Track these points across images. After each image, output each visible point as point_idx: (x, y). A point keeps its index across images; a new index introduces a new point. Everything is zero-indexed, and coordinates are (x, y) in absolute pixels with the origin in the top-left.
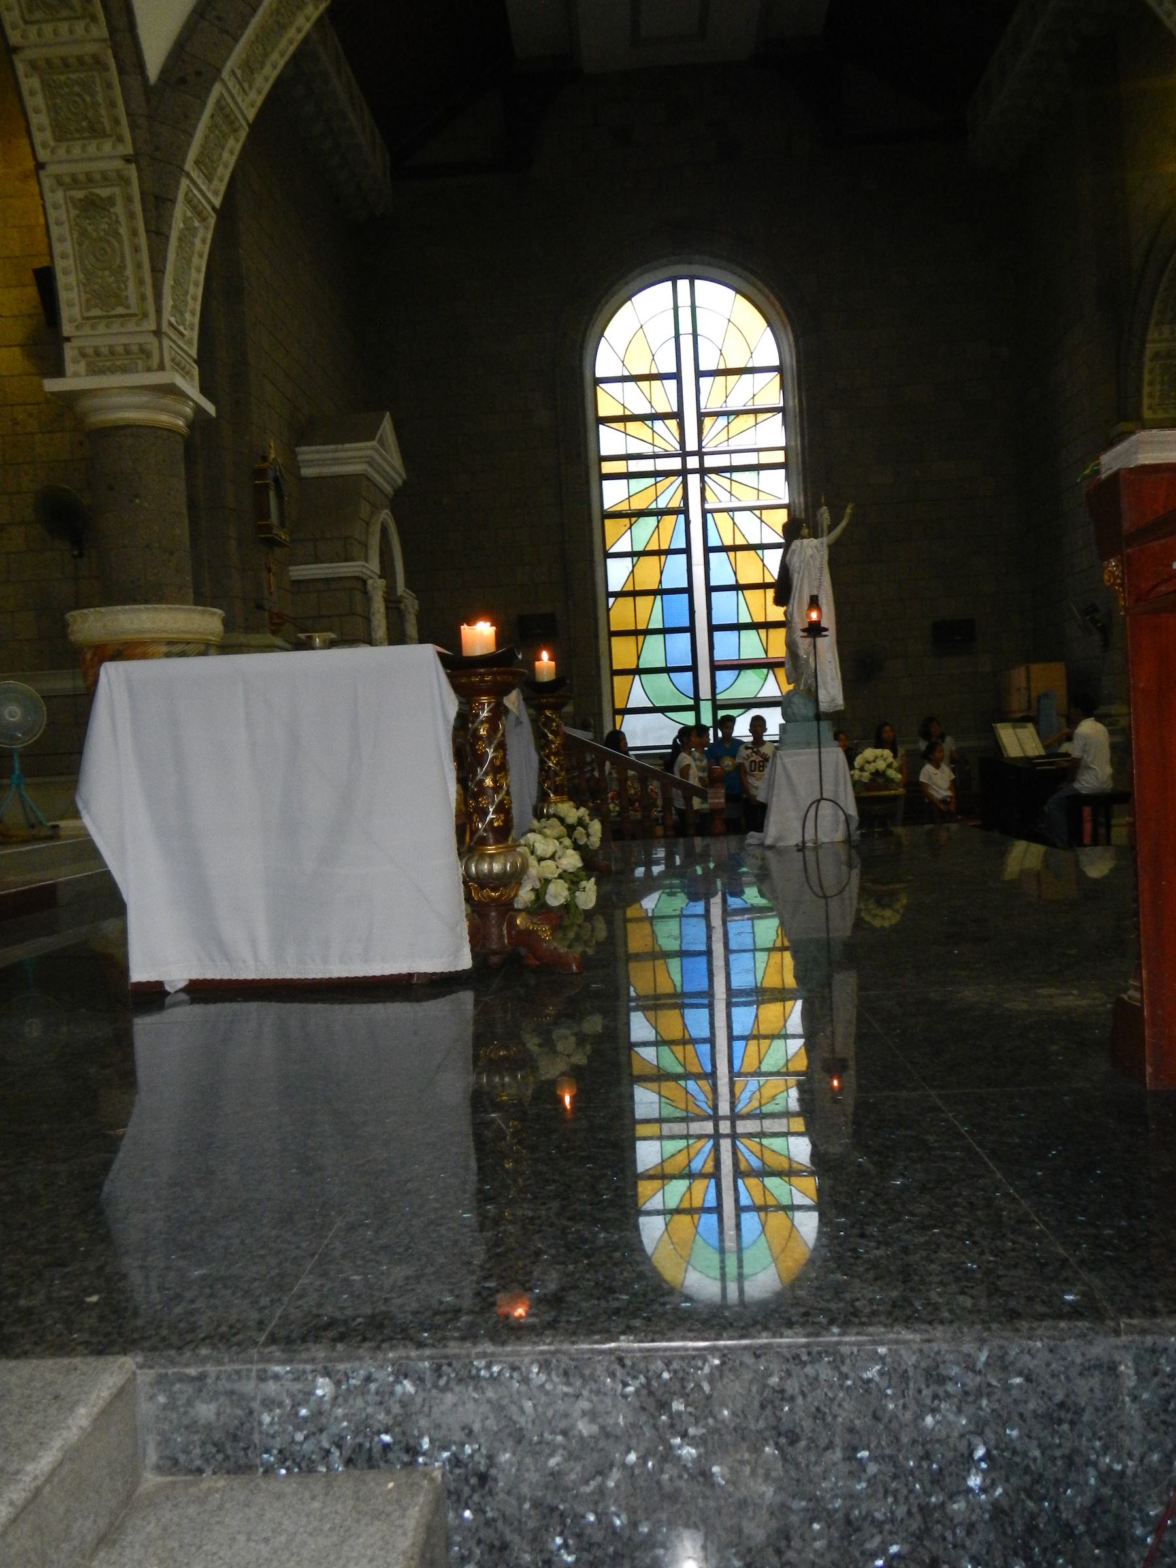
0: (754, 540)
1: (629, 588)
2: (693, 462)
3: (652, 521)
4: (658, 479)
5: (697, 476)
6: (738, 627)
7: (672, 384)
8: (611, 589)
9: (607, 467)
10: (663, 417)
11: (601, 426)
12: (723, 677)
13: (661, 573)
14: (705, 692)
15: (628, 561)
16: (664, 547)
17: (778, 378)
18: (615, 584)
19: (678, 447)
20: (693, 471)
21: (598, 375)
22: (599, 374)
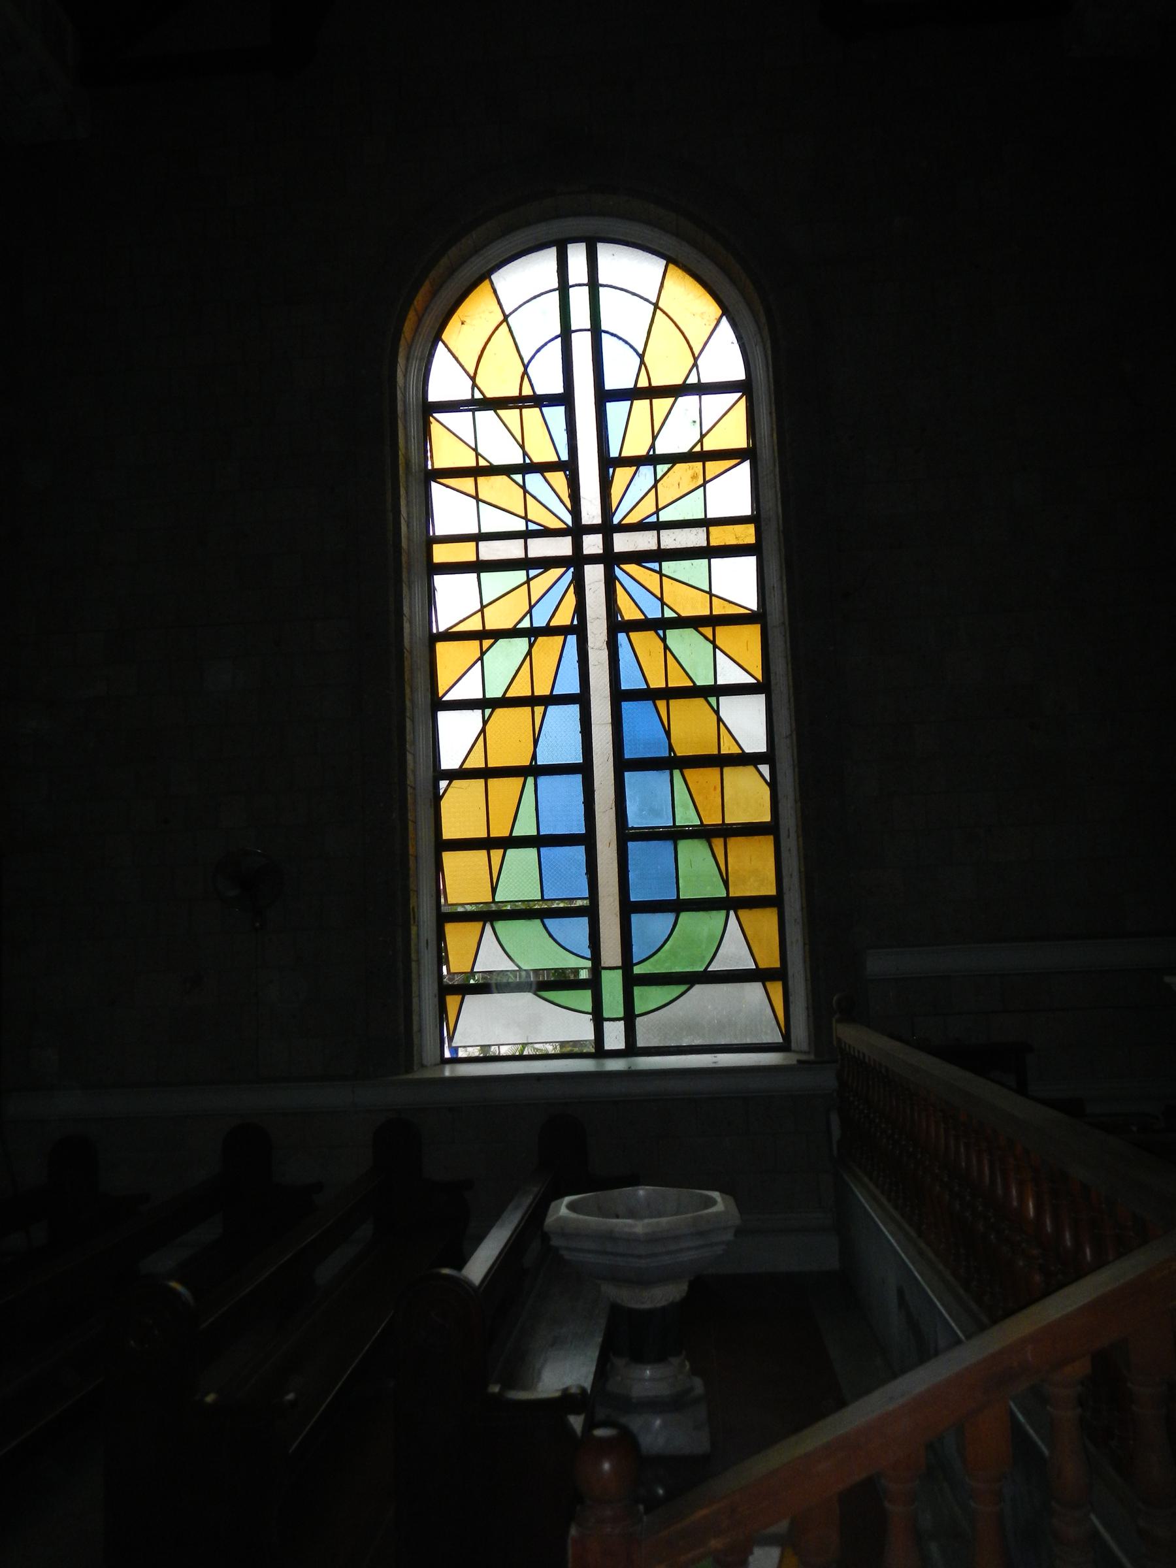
0: (703, 679)
1: (476, 762)
2: (593, 544)
3: (522, 644)
4: (532, 573)
5: (600, 568)
6: (675, 834)
7: (556, 414)
8: (445, 765)
9: (441, 554)
10: (543, 468)
11: (434, 485)
12: (648, 927)
13: (536, 742)
14: (611, 953)
15: (476, 716)
16: (542, 690)
17: (743, 403)
18: (450, 760)
19: (568, 519)
20: (593, 559)
21: (433, 397)
22: (433, 397)
